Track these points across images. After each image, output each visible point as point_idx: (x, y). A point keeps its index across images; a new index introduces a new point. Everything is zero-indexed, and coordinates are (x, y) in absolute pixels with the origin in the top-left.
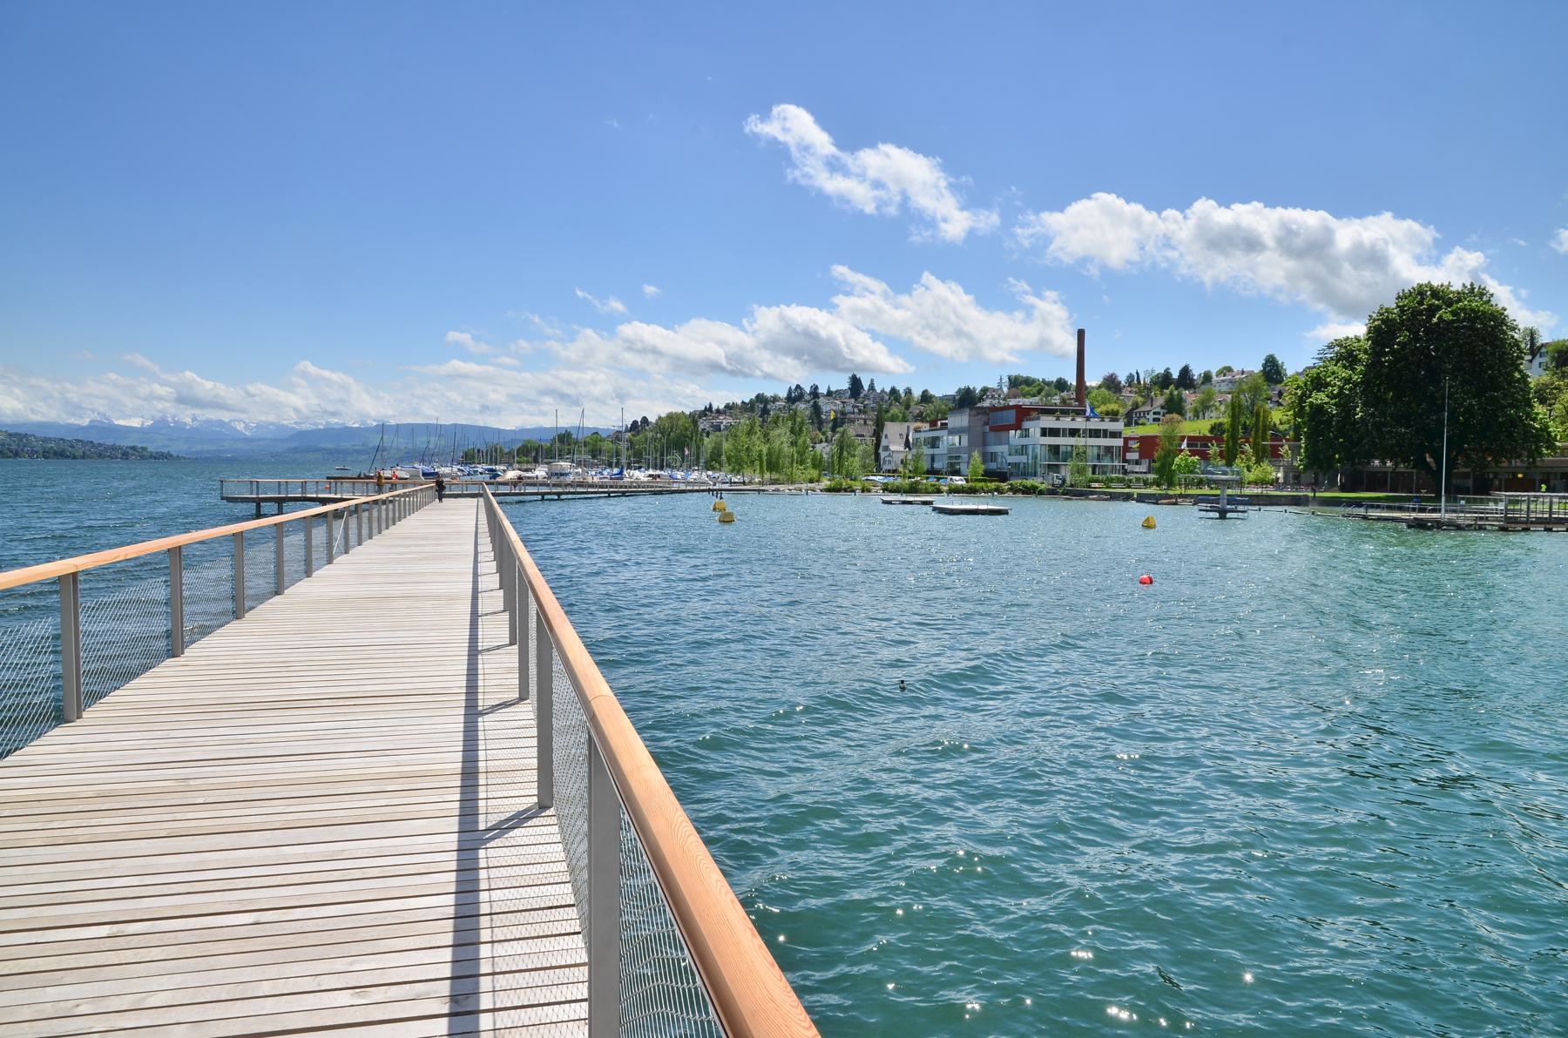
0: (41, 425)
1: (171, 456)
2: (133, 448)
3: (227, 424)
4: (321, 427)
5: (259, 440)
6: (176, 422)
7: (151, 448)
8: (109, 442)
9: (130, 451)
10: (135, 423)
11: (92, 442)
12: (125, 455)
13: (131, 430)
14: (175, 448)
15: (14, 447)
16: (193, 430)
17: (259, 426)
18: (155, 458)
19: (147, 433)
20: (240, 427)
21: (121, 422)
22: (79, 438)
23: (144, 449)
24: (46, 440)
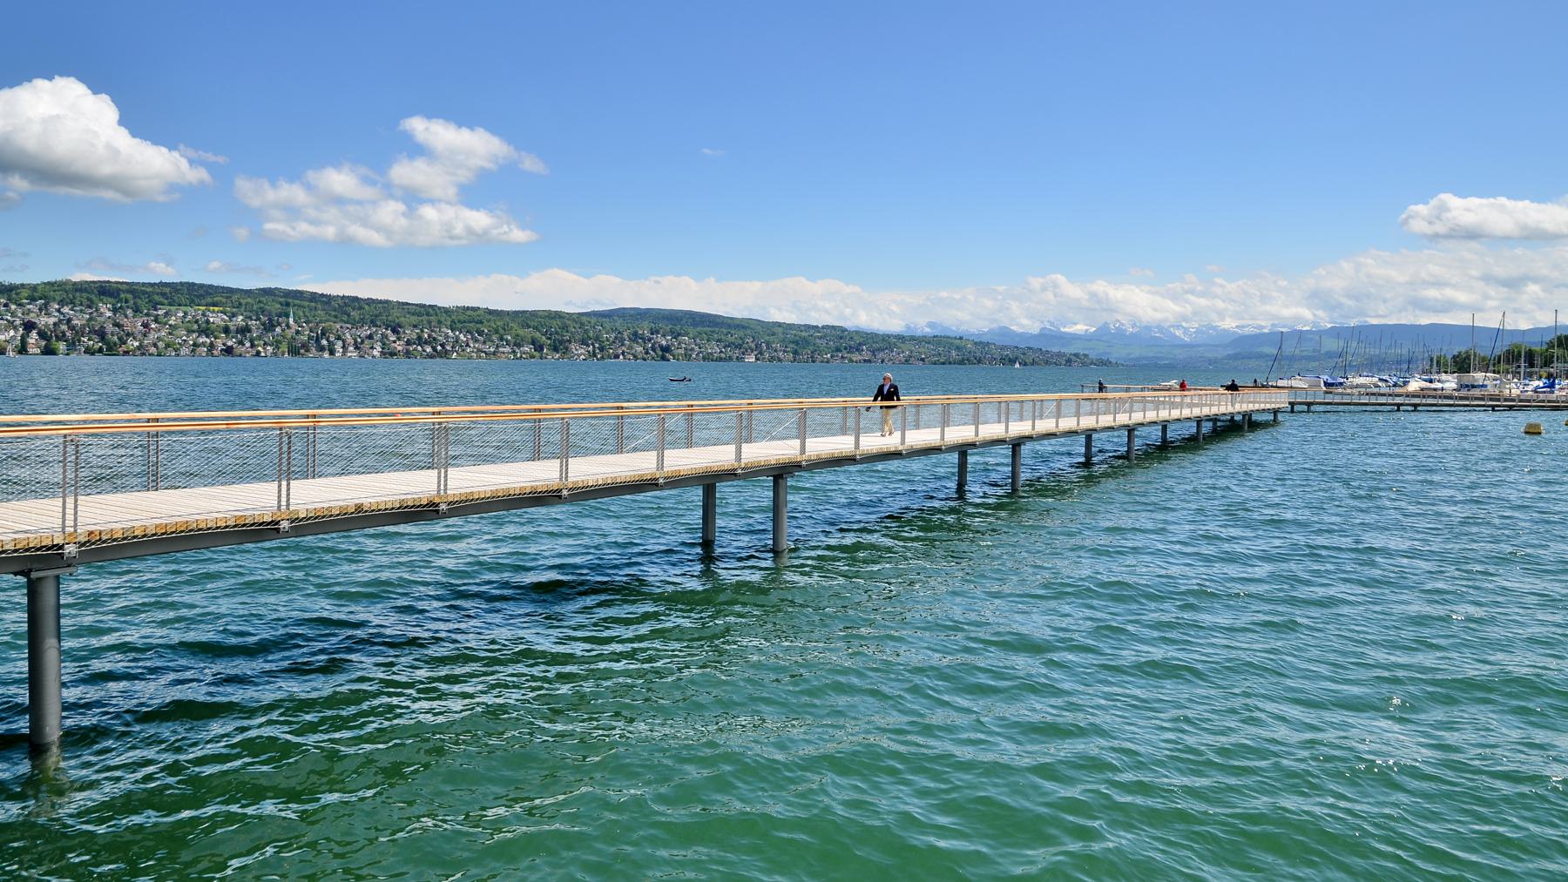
2: (1076, 355)
4: (1266, 331)
5: (1199, 346)
7: (1093, 355)
8: (1055, 350)
9: (1073, 358)
10: (1080, 328)
12: (1069, 361)
13: (1075, 337)
14: (1116, 354)
15: (978, 355)
17: (1198, 331)
19: (1090, 340)
21: (1066, 330)
23: (1086, 356)
24: (1003, 348)
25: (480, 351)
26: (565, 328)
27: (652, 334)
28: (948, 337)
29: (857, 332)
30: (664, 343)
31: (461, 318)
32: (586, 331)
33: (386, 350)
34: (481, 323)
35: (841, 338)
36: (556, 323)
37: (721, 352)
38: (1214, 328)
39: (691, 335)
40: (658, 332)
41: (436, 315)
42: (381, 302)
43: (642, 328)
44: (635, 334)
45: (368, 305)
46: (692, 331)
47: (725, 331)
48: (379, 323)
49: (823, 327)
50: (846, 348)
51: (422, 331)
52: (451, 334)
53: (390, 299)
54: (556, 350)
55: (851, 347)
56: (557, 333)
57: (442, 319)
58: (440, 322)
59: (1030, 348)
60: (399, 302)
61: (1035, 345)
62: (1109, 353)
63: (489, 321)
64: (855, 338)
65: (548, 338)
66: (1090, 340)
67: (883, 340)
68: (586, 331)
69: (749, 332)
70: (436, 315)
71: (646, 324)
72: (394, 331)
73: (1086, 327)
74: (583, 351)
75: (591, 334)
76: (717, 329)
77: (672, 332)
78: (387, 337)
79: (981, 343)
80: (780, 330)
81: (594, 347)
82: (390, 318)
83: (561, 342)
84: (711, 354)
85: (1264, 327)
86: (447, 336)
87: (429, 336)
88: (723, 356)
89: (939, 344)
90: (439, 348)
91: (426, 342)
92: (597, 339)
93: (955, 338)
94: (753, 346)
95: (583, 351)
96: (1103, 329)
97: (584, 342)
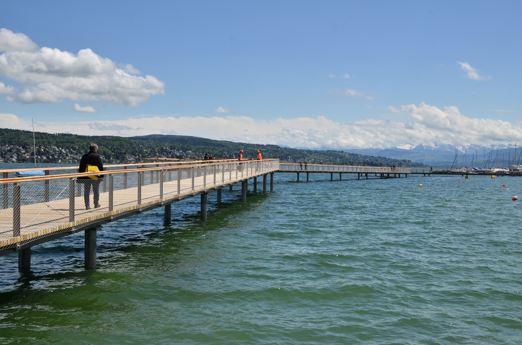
0: (365, 150)
1: (422, 165)
2: (404, 161)
3: (453, 147)
4: (506, 148)
7: (414, 161)
8: (393, 158)
9: (403, 162)
10: (407, 147)
11: (385, 158)
15: (351, 161)
16: (435, 150)
17: (470, 148)
18: (414, 166)
19: (413, 153)
23: (409, 161)
24: (365, 157)
25: (74, 158)
26: (122, 145)
27: (171, 149)
28: (335, 151)
30: (178, 154)
31: (62, 140)
32: (134, 148)
33: (20, 158)
34: (74, 143)
35: (277, 152)
36: (116, 143)
39: (193, 150)
40: (174, 148)
41: (47, 138)
42: (13, 131)
43: (165, 146)
44: (162, 149)
45: (6, 132)
46: (194, 148)
48: (13, 143)
49: (267, 146)
51: (40, 148)
52: (57, 149)
53: (19, 129)
54: (117, 158)
55: (282, 157)
56: (117, 149)
57: (51, 141)
58: (49, 143)
59: (379, 157)
60: (23, 131)
61: (382, 156)
63: (78, 142)
64: (285, 151)
65: (113, 152)
66: (413, 153)
67: (300, 152)
68: (134, 148)
69: (225, 148)
70: (47, 138)
71: (167, 144)
72: (24, 148)
74: (133, 159)
75: (137, 149)
76: (208, 147)
77: (182, 148)
78: (20, 151)
79: (353, 154)
80: (243, 147)
81: (139, 157)
82: (20, 140)
83: (121, 154)
85: (505, 146)
86: (54, 150)
87: (44, 150)
89: (330, 155)
90: (51, 157)
91: (43, 154)
92: (141, 152)
93: (339, 152)
95: (133, 159)
96: (420, 147)
97: (133, 154)
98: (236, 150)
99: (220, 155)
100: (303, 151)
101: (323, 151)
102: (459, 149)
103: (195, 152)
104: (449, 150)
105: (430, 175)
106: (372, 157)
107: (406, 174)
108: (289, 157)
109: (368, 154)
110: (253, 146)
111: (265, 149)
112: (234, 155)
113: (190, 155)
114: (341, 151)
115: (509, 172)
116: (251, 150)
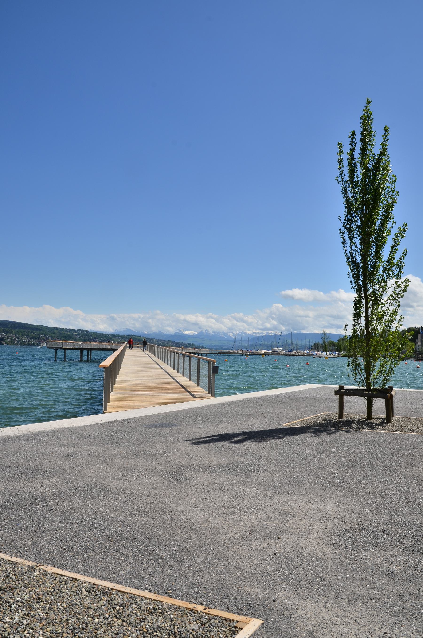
2: (189, 344)
4: (264, 335)
6: (206, 333)
7: (196, 344)
8: (181, 342)
13: (189, 336)
19: (195, 338)
20: (231, 335)
22: (170, 340)
23: (193, 344)
28: (135, 336)
29: (94, 333)
35: (86, 335)
37: (29, 341)
38: (245, 333)
46: (13, 330)
47: (30, 331)
49: (78, 330)
50: (88, 340)
55: (91, 340)
59: (170, 341)
62: (203, 343)
66: (195, 338)
69: (42, 332)
73: (194, 332)
80: (57, 331)
84: (24, 342)
85: (264, 333)
88: (30, 342)
93: (138, 336)
94: (45, 338)
96: (201, 333)
98: (52, 333)
99: (37, 338)
100: (108, 335)
101: (125, 335)
102: (231, 336)
103: (15, 334)
104: (223, 336)
105: (221, 354)
106: (164, 340)
107: (206, 354)
108: (97, 340)
109: (161, 338)
110: (66, 330)
111: (76, 333)
112: (49, 338)
113: (11, 337)
114: (139, 336)
115: (272, 353)
116: (65, 334)
